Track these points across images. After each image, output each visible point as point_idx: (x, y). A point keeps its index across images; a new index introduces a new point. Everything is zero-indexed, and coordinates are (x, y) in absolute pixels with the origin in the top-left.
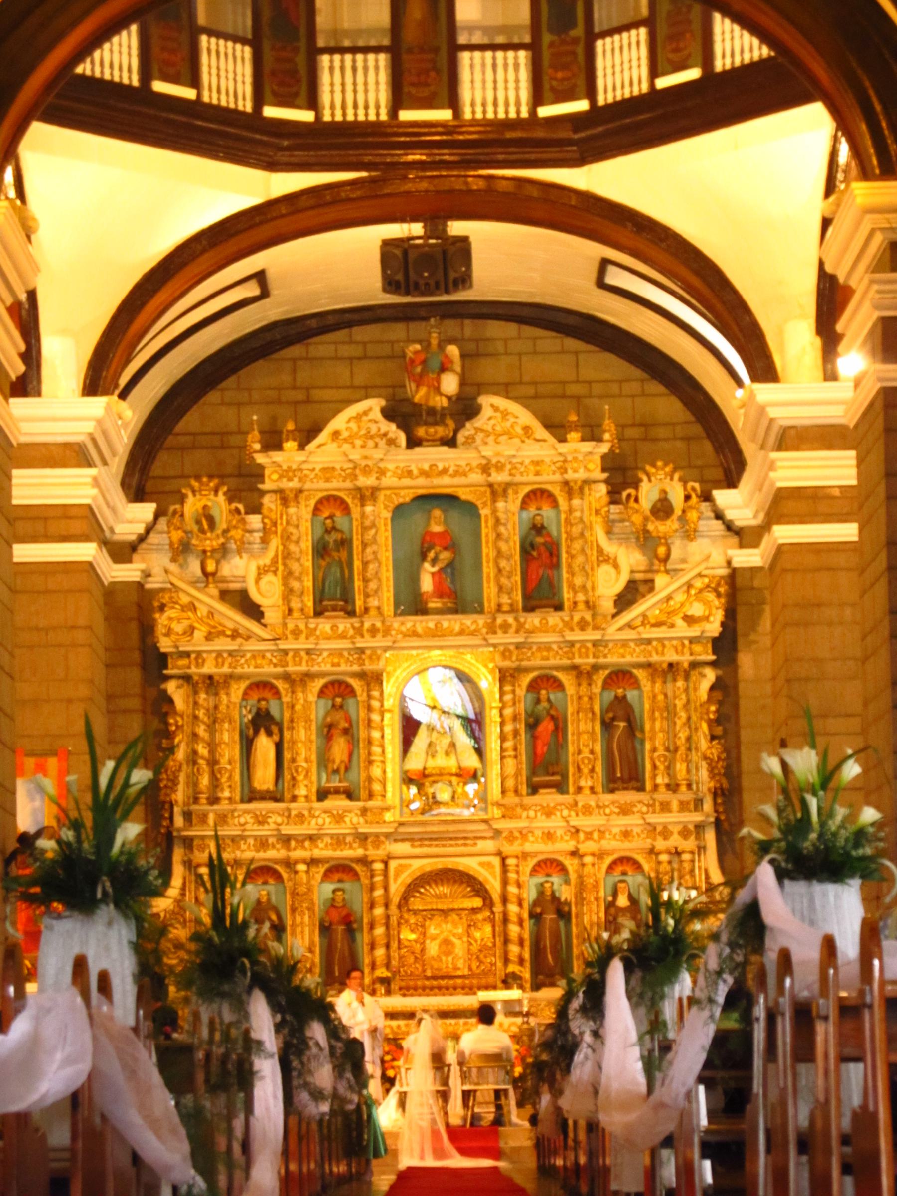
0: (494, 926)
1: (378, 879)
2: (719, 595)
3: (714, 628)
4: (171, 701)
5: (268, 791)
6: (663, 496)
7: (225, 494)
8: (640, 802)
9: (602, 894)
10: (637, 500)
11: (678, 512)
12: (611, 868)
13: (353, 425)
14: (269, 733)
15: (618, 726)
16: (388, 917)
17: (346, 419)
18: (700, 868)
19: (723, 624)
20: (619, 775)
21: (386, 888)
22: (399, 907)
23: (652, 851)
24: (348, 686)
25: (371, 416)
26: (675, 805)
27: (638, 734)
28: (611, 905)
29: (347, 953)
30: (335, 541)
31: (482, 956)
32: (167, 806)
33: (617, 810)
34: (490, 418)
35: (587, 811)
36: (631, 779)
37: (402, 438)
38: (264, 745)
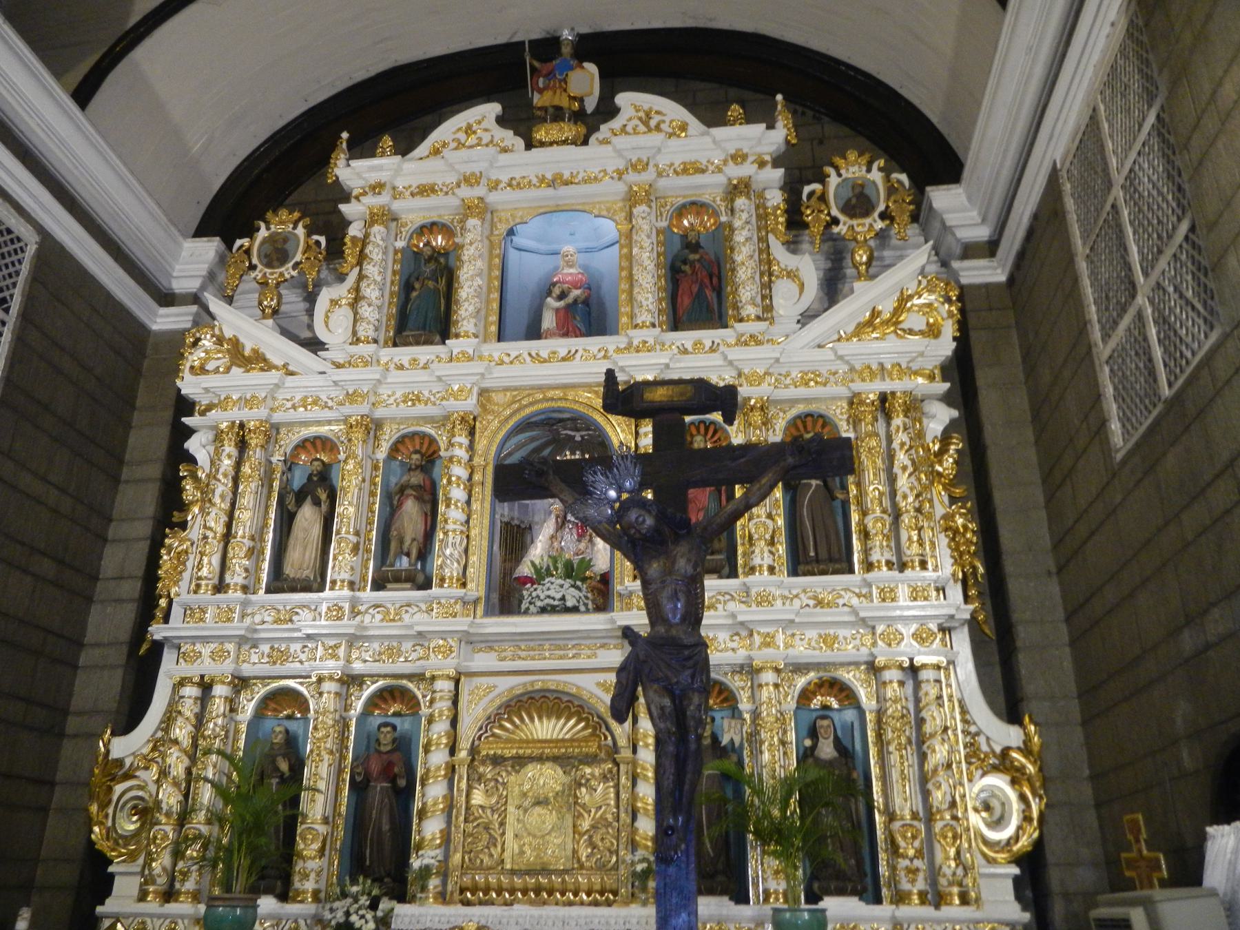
0: (617, 786)
1: (444, 705)
2: (948, 300)
3: (945, 347)
4: (192, 460)
5: (307, 579)
6: (857, 190)
7: (305, 227)
8: (846, 590)
9: (792, 736)
10: (823, 198)
11: (882, 207)
12: (805, 696)
13: (462, 136)
14: (317, 503)
15: (810, 485)
16: (451, 769)
17: (454, 129)
18: (950, 697)
19: (955, 339)
20: (812, 554)
21: (454, 722)
22: (473, 751)
23: (873, 669)
24: (432, 441)
25: (484, 125)
26: (903, 592)
27: (840, 495)
28: (806, 756)
29: (386, 827)
30: (434, 272)
31: (597, 839)
32: (163, 602)
33: (812, 603)
34: (630, 119)
35: (764, 600)
36: (831, 560)
37: (520, 143)
38: (308, 517)
